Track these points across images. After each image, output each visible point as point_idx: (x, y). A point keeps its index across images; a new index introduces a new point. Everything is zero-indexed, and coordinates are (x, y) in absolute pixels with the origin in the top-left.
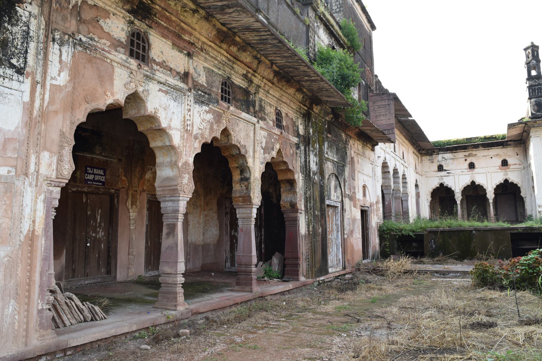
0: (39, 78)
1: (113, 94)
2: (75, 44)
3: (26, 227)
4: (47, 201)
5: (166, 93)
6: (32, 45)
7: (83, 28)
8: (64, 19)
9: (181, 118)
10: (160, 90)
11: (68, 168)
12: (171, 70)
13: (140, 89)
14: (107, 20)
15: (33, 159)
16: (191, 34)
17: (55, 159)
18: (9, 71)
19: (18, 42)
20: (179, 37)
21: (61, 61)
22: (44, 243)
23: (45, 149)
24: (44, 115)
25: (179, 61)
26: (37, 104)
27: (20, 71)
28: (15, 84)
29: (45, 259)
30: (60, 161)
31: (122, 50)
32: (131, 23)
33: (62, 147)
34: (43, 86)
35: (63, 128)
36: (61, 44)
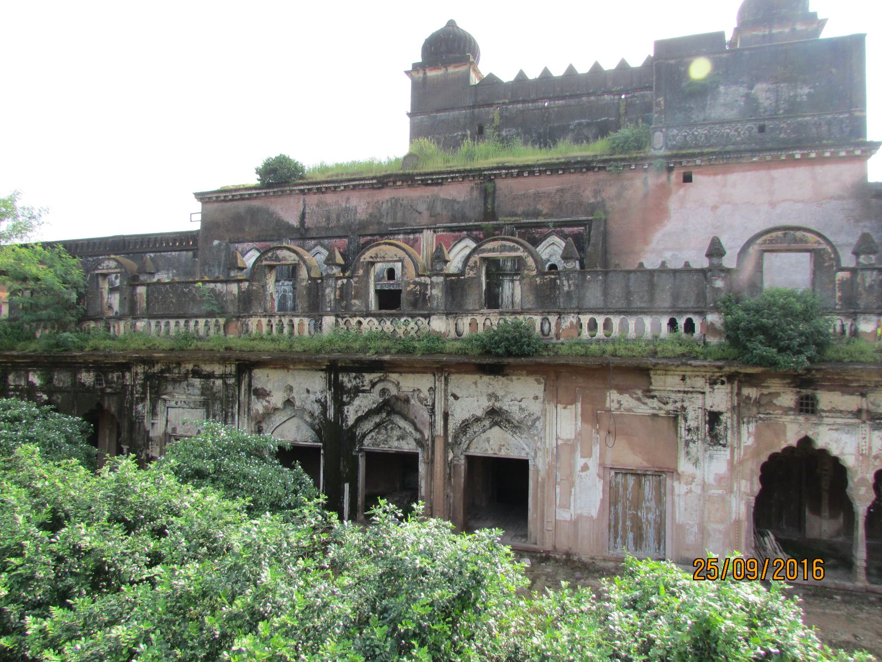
0: (735, 445)
1: (786, 441)
2: (756, 421)
3: (734, 517)
4: (748, 504)
5: (837, 430)
6: (729, 433)
7: (762, 410)
8: (749, 409)
9: (854, 445)
10: (830, 429)
11: (757, 487)
12: (841, 412)
13: (810, 434)
14: (779, 398)
15: (735, 485)
16: (858, 381)
17: (749, 483)
18: (720, 447)
19: (722, 433)
20: (848, 386)
21: (748, 433)
22: (747, 525)
23: (743, 478)
24: (741, 462)
25: (852, 402)
26: (736, 458)
27: (724, 446)
28: (722, 452)
29: (748, 532)
30: (752, 484)
31: (792, 413)
32: (798, 392)
33: (752, 477)
34: (739, 447)
35: (753, 468)
36: (748, 423)
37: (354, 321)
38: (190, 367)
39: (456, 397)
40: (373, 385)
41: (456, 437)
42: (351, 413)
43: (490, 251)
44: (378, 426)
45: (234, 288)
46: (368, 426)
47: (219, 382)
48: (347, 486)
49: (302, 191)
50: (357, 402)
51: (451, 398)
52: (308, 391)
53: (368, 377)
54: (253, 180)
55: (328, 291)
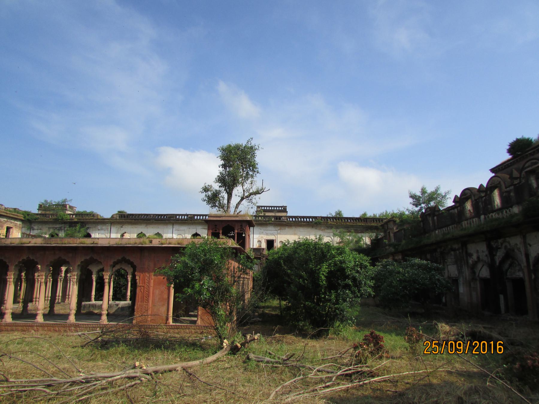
37: (490, 216)
38: (450, 247)
39: (530, 245)
40: (502, 244)
41: (534, 266)
42: (497, 260)
43: (528, 167)
44: (511, 265)
45: (456, 210)
46: (506, 266)
47: (458, 252)
48: (502, 297)
49: (530, 154)
50: (498, 254)
51: (528, 246)
52: (483, 252)
53: (500, 241)
54: (508, 157)
55: (480, 203)
